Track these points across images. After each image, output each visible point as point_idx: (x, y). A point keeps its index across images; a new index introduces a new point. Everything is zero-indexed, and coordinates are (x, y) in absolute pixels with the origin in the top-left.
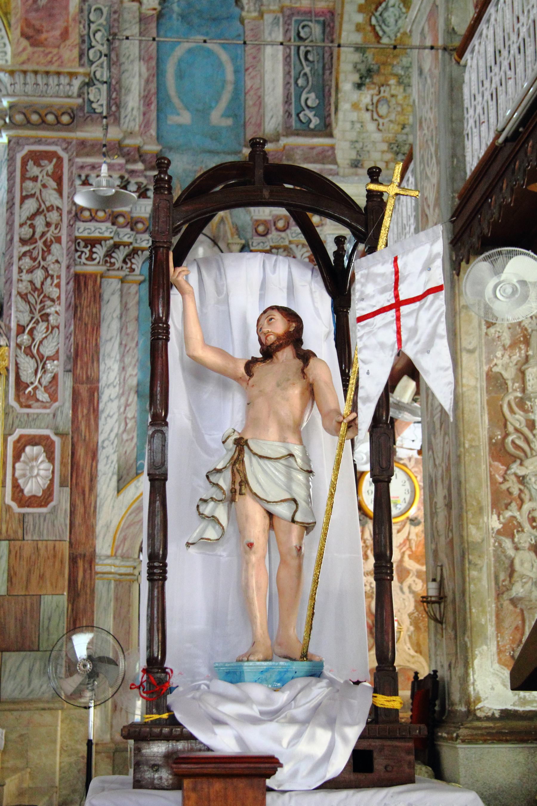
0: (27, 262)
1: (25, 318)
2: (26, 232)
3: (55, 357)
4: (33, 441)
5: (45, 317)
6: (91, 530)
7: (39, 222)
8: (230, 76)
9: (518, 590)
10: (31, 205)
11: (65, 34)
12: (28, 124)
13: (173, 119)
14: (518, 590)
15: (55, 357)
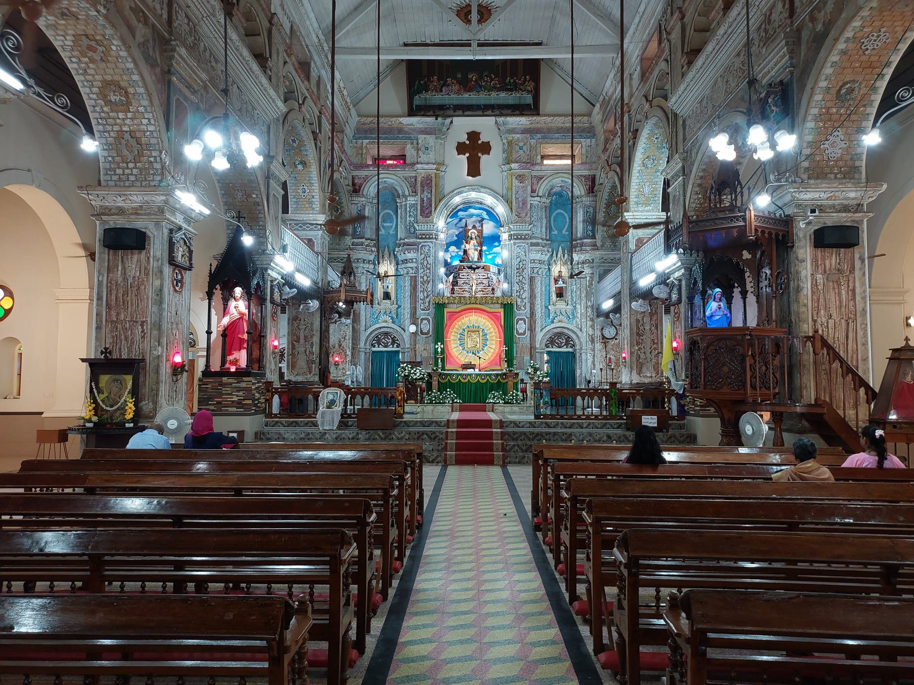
0: (518, 274)
1: (518, 289)
2: (518, 266)
3: (525, 298)
4: (521, 319)
5: (523, 288)
6: (535, 341)
7: (521, 264)
8: (568, 221)
9: (641, 361)
10: (519, 260)
11: (526, 215)
12: (517, 239)
13: (553, 233)
14: (641, 361)
15: (525, 298)
